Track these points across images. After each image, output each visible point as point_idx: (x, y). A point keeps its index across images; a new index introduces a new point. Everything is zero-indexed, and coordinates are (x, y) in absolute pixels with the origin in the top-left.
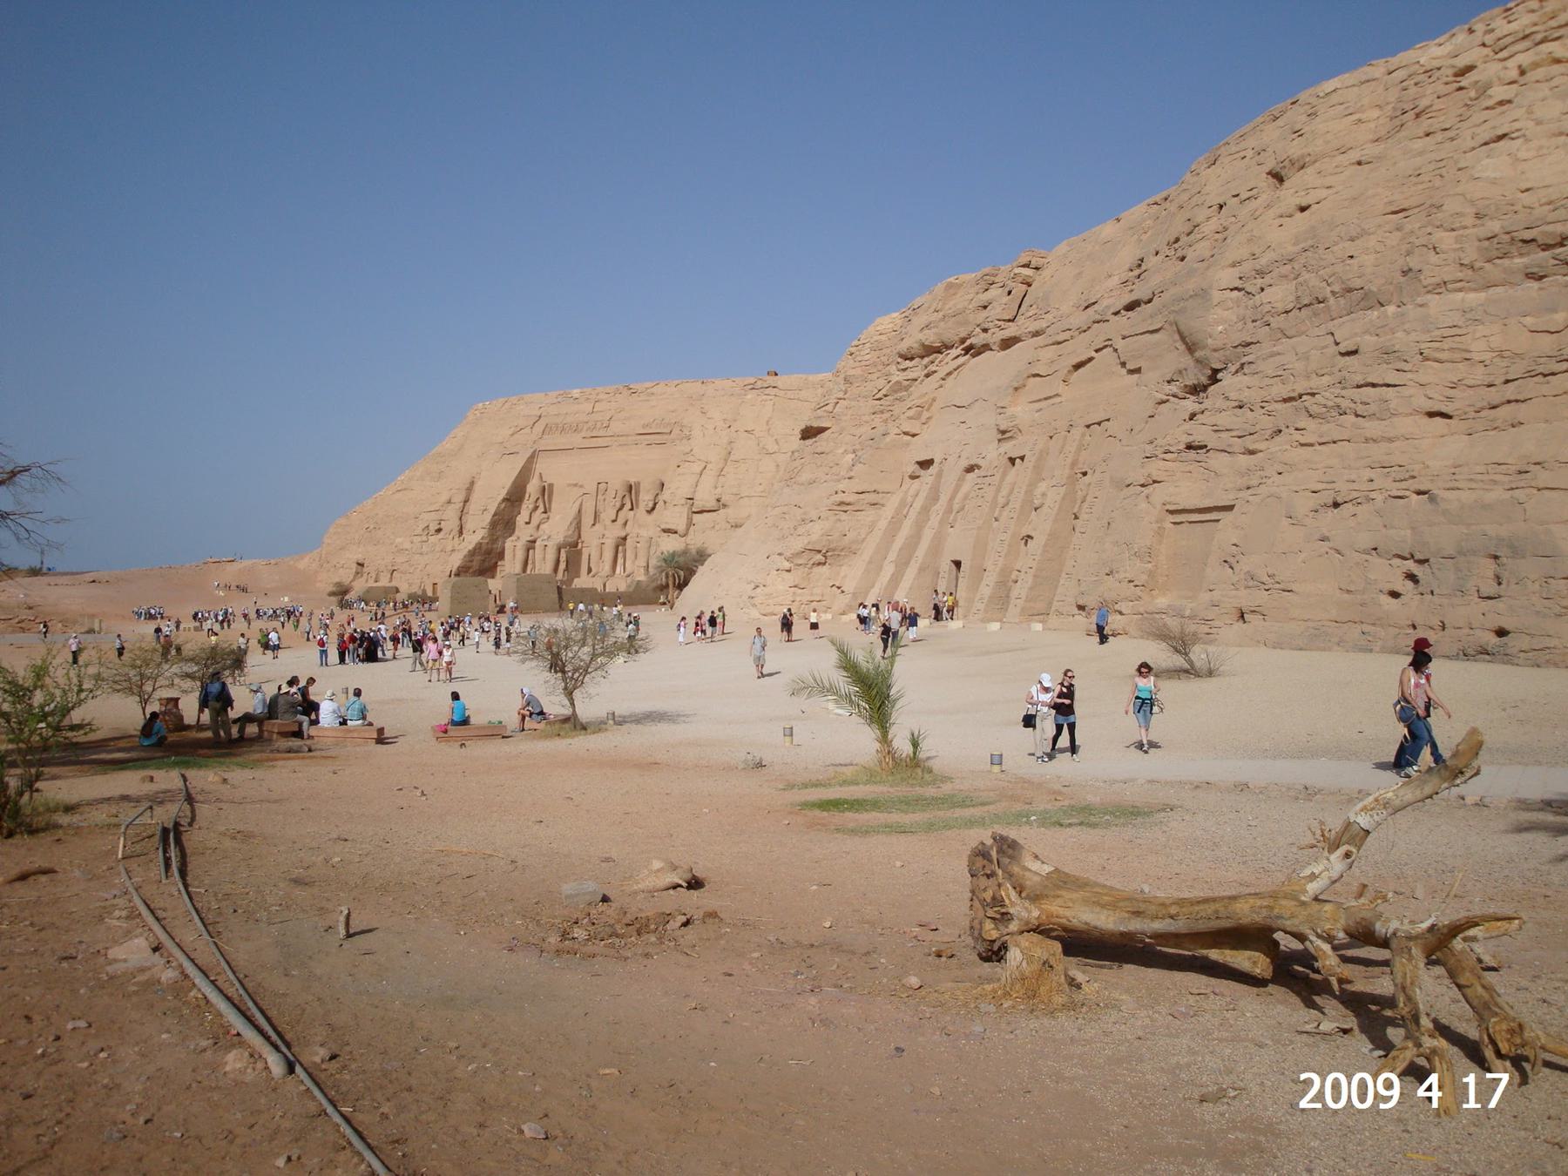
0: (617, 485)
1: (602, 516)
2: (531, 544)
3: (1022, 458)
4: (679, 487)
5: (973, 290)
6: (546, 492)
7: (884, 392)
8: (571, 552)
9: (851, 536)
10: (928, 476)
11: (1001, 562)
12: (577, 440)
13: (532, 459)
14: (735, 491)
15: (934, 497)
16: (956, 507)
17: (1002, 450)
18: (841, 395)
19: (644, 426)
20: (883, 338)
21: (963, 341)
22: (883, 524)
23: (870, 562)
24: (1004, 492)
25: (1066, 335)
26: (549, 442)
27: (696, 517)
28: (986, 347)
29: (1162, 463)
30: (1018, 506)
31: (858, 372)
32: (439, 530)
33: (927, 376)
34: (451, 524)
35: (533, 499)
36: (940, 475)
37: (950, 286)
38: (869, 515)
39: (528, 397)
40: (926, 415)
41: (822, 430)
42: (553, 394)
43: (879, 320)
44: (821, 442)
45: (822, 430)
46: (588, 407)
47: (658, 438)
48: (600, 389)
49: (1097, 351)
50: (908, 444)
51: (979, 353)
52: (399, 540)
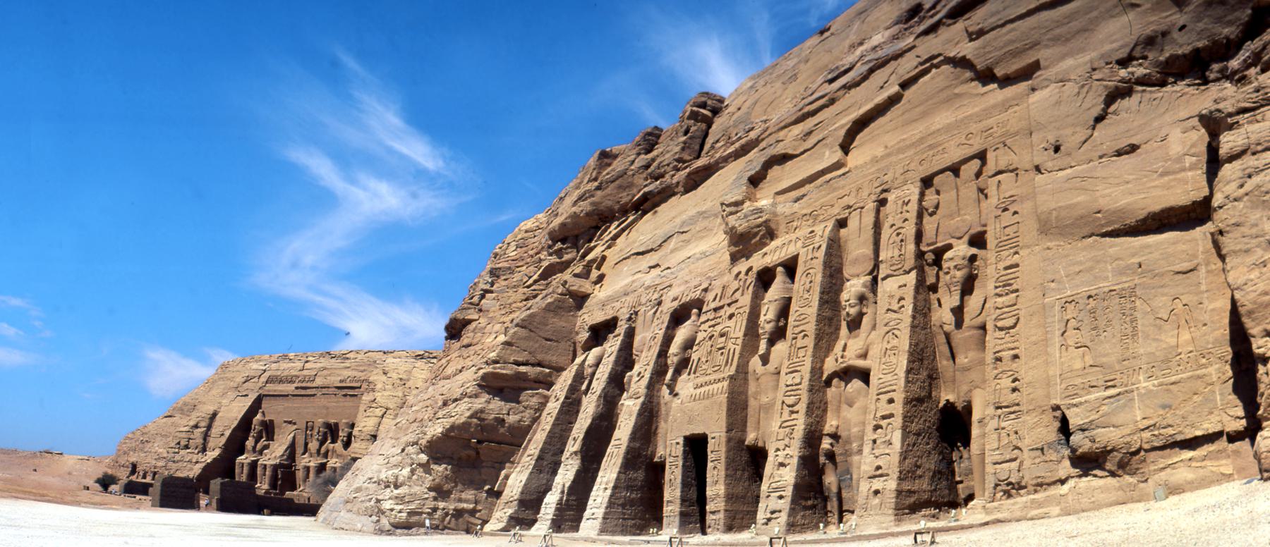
2: (254, 465)
7: (535, 277)
9: (512, 419)
10: (612, 345)
11: (800, 424)
12: (289, 388)
15: (626, 360)
16: (673, 360)
18: (488, 287)
22: (553, 407)
23: (540, 458)
30: (811, 328)
31: (506, 265)
36: (630, 334)
40: (595, 274)
44: (466, 338)
46: (299, 365)
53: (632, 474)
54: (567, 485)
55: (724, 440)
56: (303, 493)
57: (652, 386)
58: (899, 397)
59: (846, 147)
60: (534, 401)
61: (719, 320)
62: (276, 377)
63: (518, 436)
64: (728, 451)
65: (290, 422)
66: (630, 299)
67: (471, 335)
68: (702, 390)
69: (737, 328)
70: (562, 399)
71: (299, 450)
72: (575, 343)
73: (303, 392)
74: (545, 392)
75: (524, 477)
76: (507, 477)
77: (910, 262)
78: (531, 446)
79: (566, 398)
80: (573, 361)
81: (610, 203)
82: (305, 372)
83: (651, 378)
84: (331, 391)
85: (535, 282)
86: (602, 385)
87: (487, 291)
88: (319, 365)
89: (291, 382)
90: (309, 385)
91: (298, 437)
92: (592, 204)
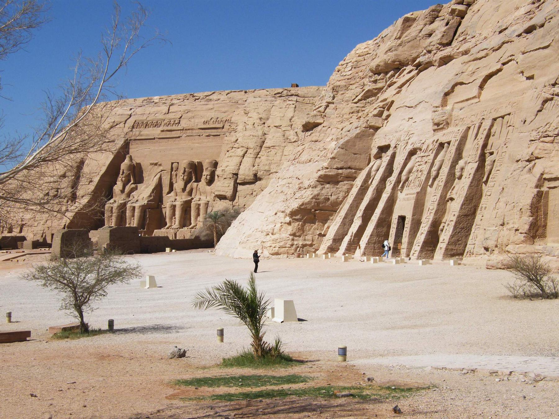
0: (184, 164)
1: (175, 186)
2: (123, 207)
3: (449, 143)
4: (227, 165)
5: (424, 22)
7: (359, 97)
8: (153, 212)
9: (333, 198)
14: (267, 168)
17: (435, 138)
18: (330, 100)
19: (205, 123)
20: (361, 58)
21: (414, 60)
22: (354, 191)
23: (345, 218)
24: (435, 168)
25: (483, 54)
27: (240, 188)
28: (429, 64)
29: (542, 144)
31: (343, 83)
33: (389, 86)
34: (66, 191)
36: (393, 156)
37: (407, 20)
38: (343, 186)
40: (386, 113)
41: (317, 125)
42: (140, 100)
43: (358, 46)
44: (316, 133)
45: (317, 125)
46: (165, 109)
47: (214, 132)
48: (173, 96)
49: (504, 64)
50: (373, 135)
51: (426, 69)
53: (380, 230)
54: (354, 233)
55: (411, 219)
56: (169, 231)
57: (394, 189)
58: (457, 214)
59: (481, 87)
60: (345, 188)
61: (422, 163)
63: (334, 208)
64: (412, 224)
65: (156, 164)
66: (397, 135)
67: (318, 134)
68: (408, 196)
69: (426, 168)
70: (359, 187)
71: (166, 189)
72: (370, 155)
73: (169, 135)
74: (352, 182)
75: (336, 228)
76: (328, 228)
77: (477, 159)
79: (361, 186)
80: (368, 164)
81: (406, 56)
82: (171, 116)
83: (394, 185)
85: (359, 100)
86: (377, 183)
87: (329, 103)
88: (183, 108)
89: (156, 124)
90: (174, 127)
91: (164, 178)
92: (396, 55)
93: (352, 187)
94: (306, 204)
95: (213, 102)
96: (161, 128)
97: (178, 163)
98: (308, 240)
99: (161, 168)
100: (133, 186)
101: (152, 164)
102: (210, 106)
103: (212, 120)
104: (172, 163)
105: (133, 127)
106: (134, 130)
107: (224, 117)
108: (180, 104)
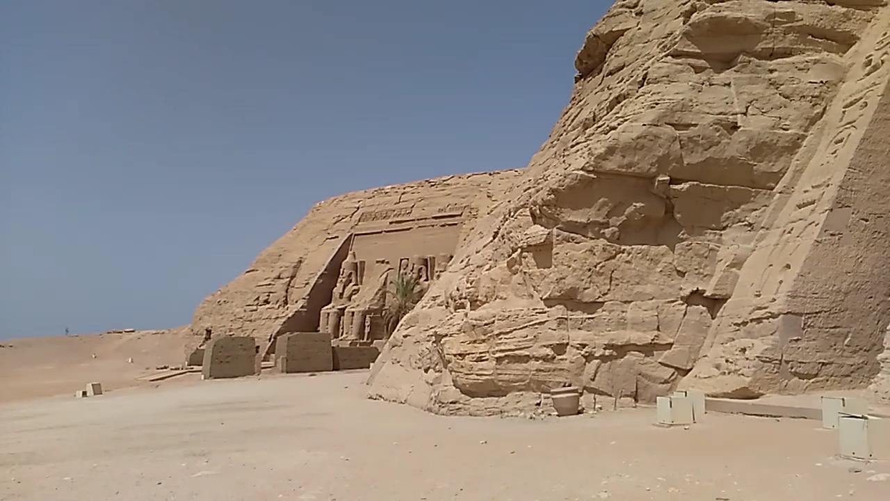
0: (415, 257)
6: (359, 269)
9: (755, 125)
12: (384, 224)
13: (348, 241)
19: (440, 211)
23: (840, 203)
26: (364, 227)
32: (267, 302)
35: (347, 272)
38: (804, 71)
39: (350, 194)
47: (450, 221)
52: (238, 310)
62: (370, 213)
65: (383, 262)
73: (399, 227)
76: (737, 264)
78: (805, 183)
84: (428, 222)
93: (842, 81)
94: (629, 149)
95: (450, 187)
96: (390, 220)
97: (408, 259)
98: (638, 324)
99: (389, 266)
100: (356, 287)
101: (377, 262)
102: (447, 192)
103: (450, 207)
104: (401, 260)
105: (359, 221)
106: (360, 223)
107: (464, 202)
108: (413, 191)
